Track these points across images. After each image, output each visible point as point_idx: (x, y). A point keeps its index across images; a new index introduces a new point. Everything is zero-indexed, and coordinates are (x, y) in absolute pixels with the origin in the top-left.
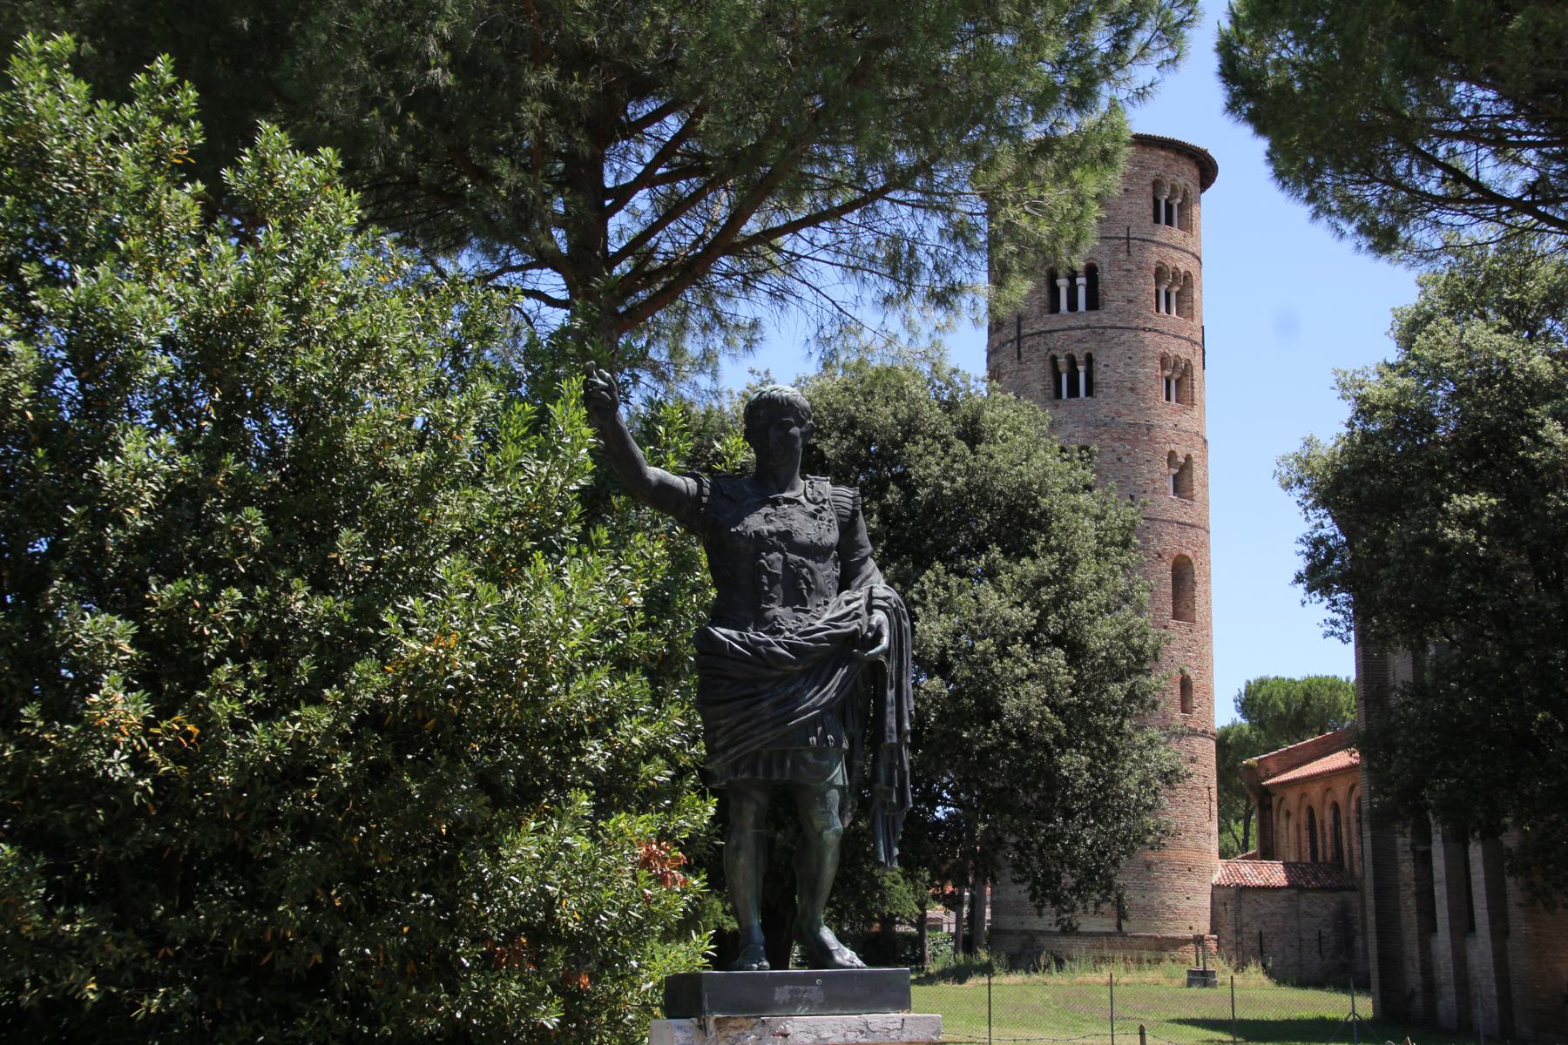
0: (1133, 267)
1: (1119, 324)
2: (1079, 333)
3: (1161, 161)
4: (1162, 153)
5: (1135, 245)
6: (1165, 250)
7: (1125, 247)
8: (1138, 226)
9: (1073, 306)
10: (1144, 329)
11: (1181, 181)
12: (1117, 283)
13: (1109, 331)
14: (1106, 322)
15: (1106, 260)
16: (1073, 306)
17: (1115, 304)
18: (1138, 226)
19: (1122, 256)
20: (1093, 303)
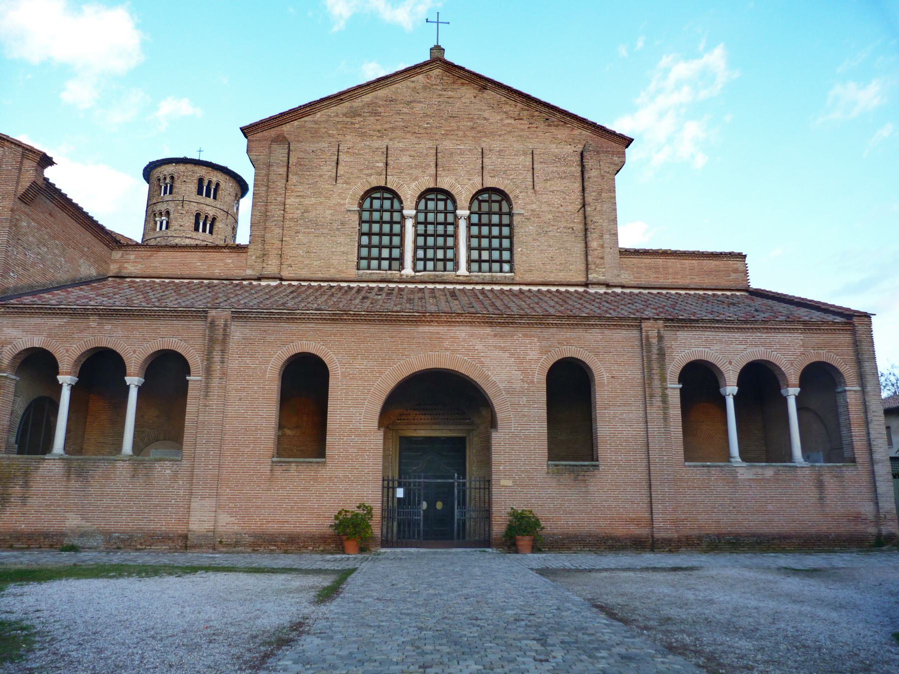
0: (184, 212)
1: (175, 235)
2: (159, 239)
3: (204, 171)
4: (204, 167)
5: (185, 203)
6: (202, 205)
7: (181, 204)
8: (188, 196)
9: (161, 229)
10: (186, 237)
11: (214, 180)
12: (176, 219)
13: (170, 238)
14: (169, 234)
15: (173, 209)
16: (161, 229)
17: (174, 227)
18: (188, 196)
19: (179, 208)
20: (167, 228)
